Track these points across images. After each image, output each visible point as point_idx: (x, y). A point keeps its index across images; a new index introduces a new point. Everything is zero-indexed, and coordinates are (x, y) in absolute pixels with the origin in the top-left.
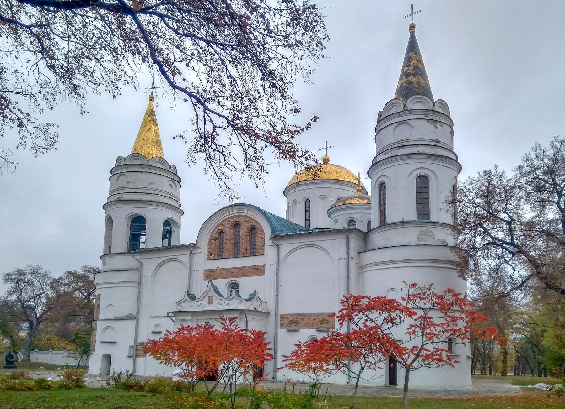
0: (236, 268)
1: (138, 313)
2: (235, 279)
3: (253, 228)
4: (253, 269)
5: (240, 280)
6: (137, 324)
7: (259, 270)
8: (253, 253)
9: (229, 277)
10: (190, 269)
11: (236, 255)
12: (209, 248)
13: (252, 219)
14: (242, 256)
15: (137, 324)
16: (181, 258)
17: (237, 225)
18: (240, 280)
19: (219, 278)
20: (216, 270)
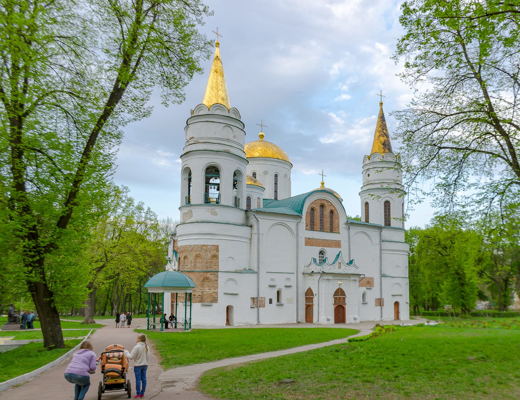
0: (324, 240)
1: (258, 268)
2: (325, 248)
3: (332, 212)
4: (334, 242)
5: (327, 250)
6: (258, 278)
7: (337, 244)
8: (331, 231)
9: (320, 246)
10: (297, 235)
11: (322, 229)
12: (306, 220)
13: (332, 205)
14: (327, 231)
15: (258, 278)
16: (289, 224)
17: (322, 206)
18: (327, 250)
19: (314, 246)
20: (312, 239)
